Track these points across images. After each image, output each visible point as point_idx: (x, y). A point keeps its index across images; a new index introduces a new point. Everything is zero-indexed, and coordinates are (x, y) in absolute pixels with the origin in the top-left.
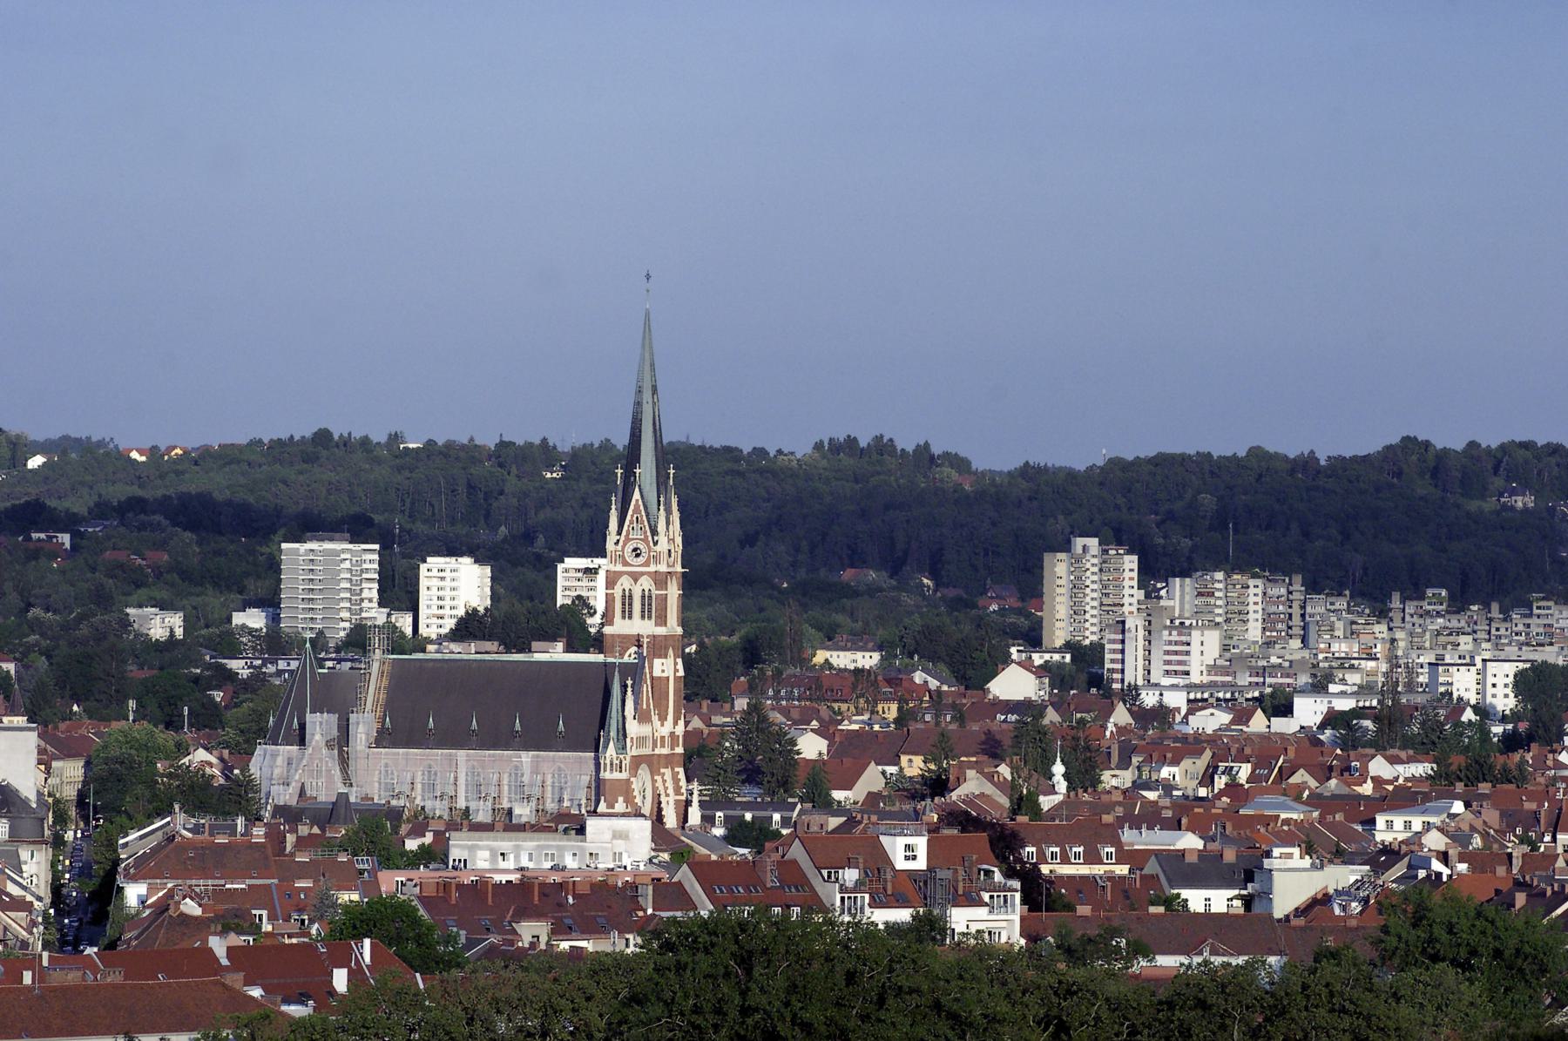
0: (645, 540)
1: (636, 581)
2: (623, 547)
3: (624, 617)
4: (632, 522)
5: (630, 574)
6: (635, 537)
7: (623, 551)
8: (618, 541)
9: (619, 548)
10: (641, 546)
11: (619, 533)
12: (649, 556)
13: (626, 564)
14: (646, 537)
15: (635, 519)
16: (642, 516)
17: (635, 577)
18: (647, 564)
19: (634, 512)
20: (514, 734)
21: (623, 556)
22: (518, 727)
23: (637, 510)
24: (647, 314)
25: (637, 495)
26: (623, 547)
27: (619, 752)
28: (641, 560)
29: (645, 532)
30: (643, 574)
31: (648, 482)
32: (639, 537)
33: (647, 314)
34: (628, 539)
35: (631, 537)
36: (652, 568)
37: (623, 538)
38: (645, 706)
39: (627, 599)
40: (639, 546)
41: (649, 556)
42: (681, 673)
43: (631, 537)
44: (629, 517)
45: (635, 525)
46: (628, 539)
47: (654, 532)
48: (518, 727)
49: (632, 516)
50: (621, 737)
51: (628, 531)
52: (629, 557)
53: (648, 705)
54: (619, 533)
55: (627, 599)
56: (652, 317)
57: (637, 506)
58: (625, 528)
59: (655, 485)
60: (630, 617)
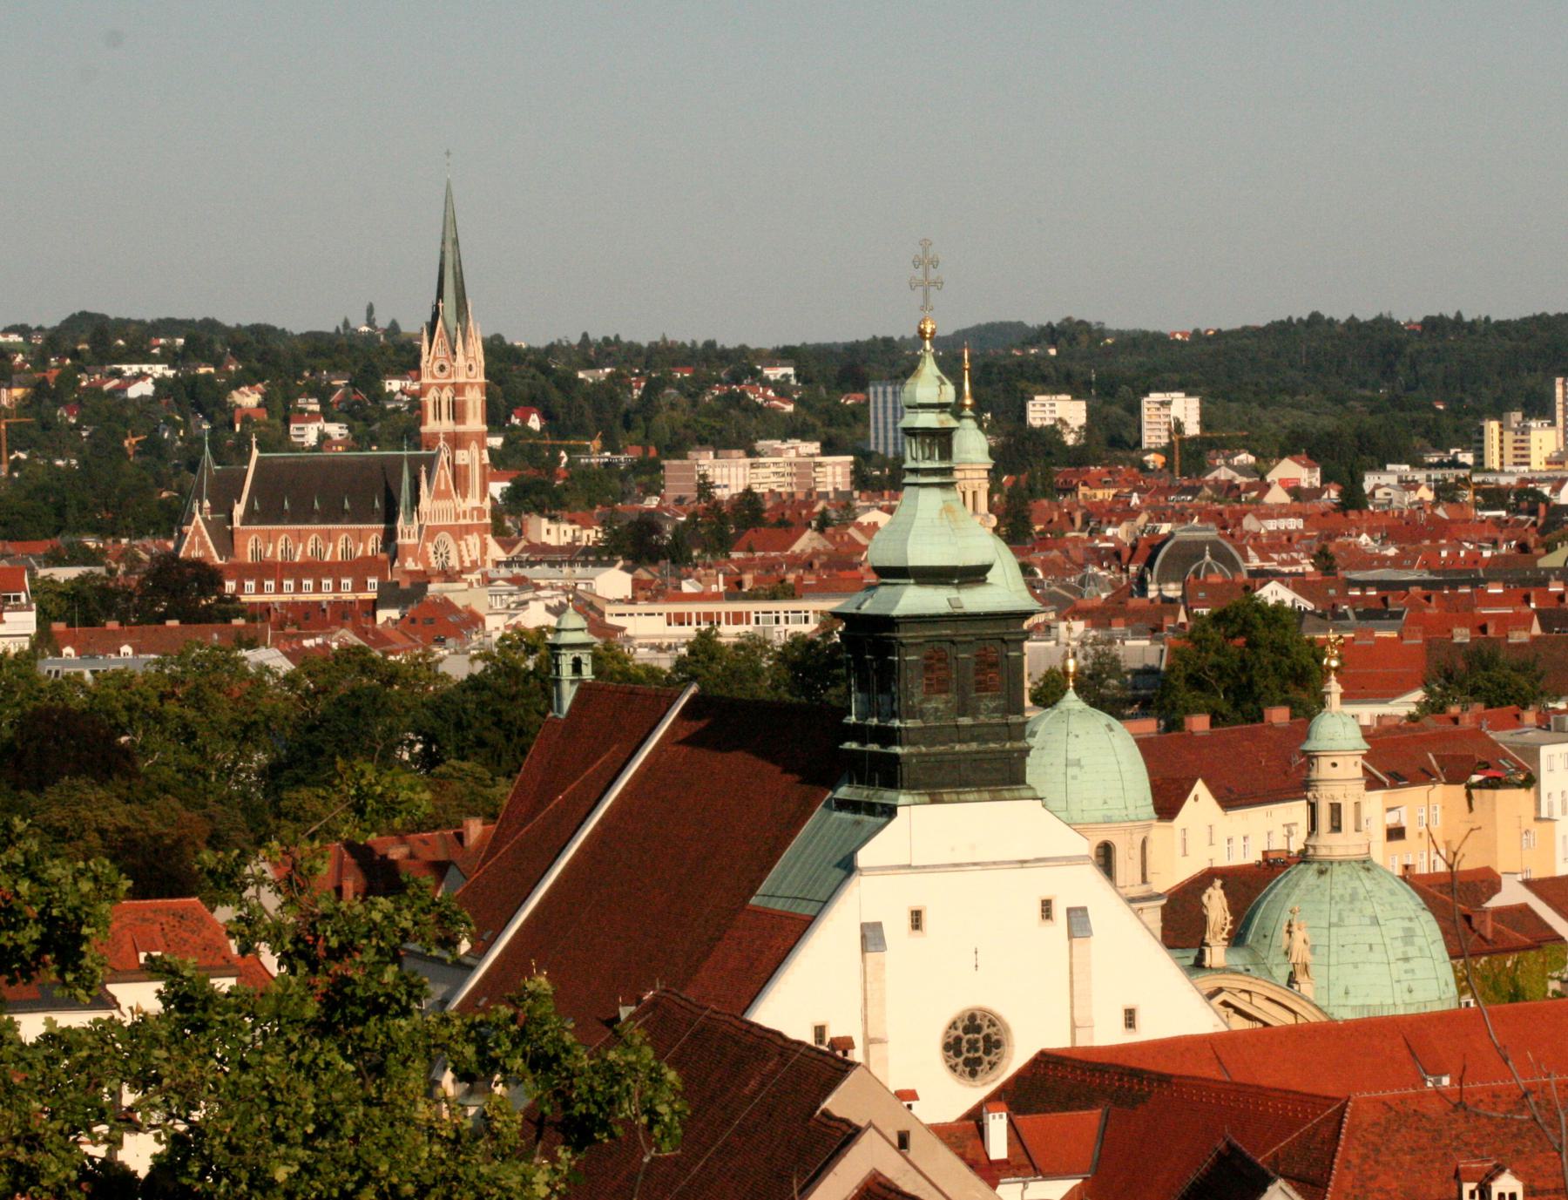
0: (447, 358)
1: (442, 389)
5: (438, 385)
10: (446, 363)
17: (441, 387)
18: (450, 376)
22: (347, 505)
24: (448, 188)
28: (445, 373)
30: (445, 384)
33: (448, 188)
34: (435, 358)
36: (452, 380)
39: (437, 404)
42: (487, 460)
46: (435, 358)
47: (454, 353)
55: (437, 404)
56: (454, 188)
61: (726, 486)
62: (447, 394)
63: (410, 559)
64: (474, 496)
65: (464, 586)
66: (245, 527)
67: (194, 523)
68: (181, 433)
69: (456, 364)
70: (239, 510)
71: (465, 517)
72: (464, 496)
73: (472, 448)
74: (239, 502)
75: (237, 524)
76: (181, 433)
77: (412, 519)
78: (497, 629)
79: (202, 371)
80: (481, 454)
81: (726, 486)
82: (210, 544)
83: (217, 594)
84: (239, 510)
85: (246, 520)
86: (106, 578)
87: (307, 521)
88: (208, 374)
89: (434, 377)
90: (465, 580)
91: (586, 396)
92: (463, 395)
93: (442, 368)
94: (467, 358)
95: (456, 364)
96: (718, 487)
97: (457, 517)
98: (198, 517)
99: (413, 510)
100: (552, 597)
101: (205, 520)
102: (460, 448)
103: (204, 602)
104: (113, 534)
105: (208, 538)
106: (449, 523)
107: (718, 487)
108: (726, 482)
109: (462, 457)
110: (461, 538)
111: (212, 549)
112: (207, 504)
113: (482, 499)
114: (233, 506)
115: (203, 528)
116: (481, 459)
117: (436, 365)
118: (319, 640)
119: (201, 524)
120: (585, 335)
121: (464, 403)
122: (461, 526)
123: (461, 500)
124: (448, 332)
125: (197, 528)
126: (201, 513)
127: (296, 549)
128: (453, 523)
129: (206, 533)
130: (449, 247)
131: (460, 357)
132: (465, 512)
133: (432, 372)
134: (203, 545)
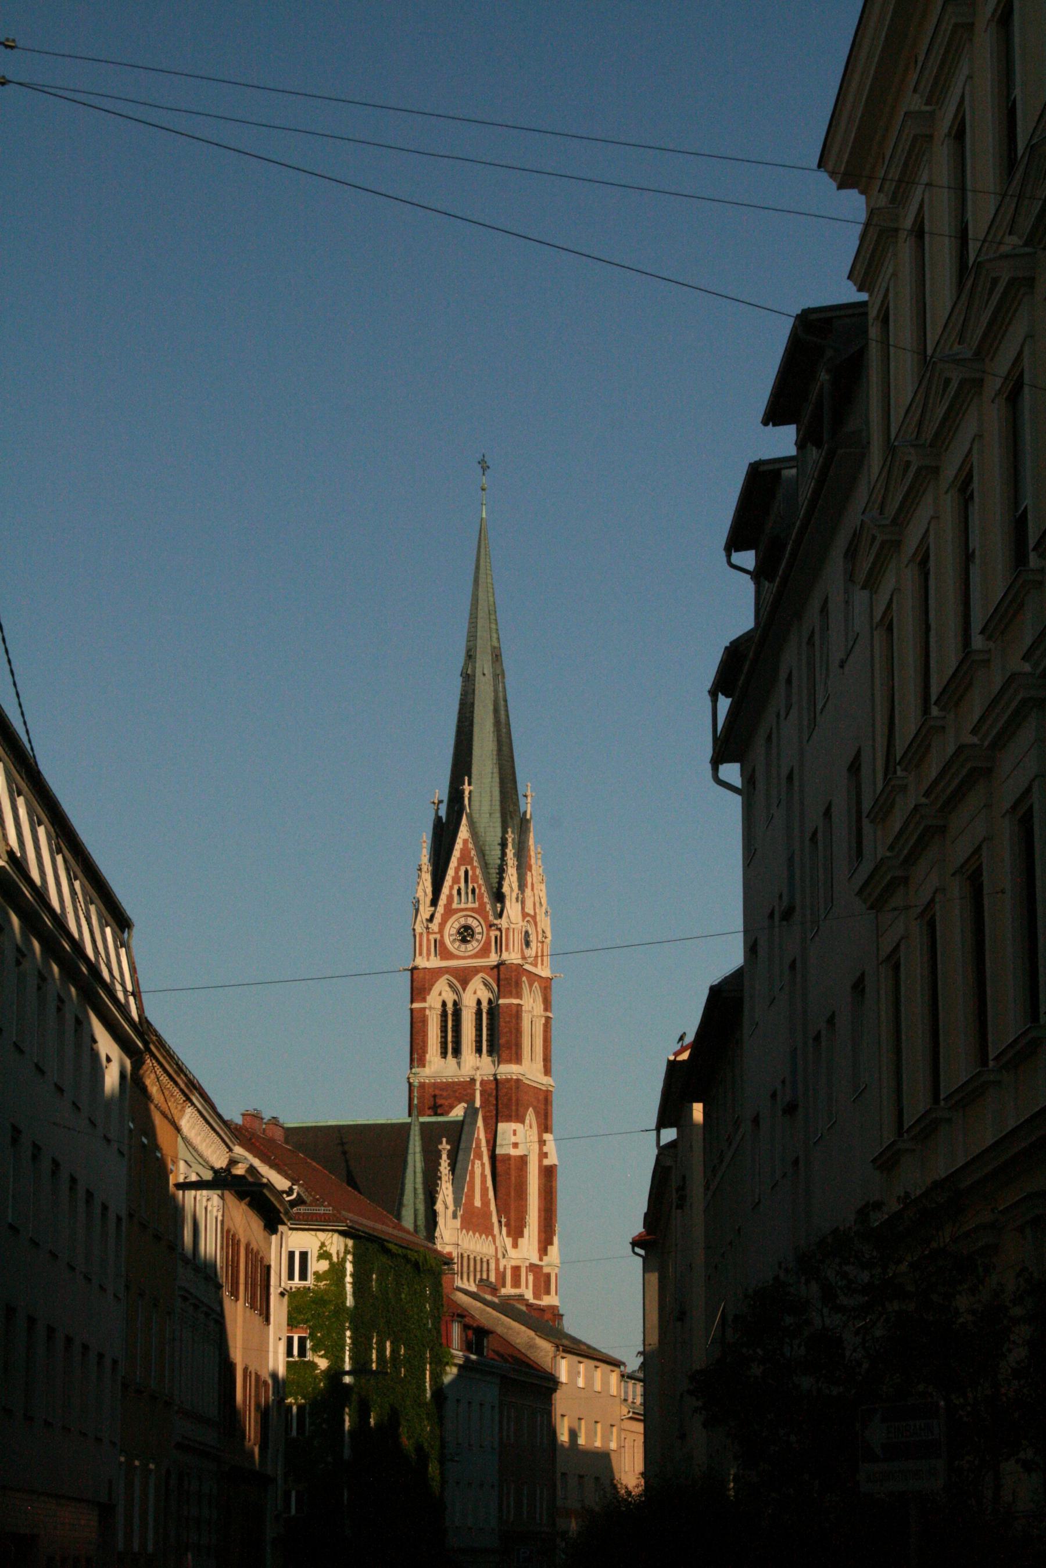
0: (481, 911)
1: (464, 983)
2: (442, 925)
4: (456, 880)
6: (463, 906)
7: (441, 931)
8: (432, 917)
9: (434, 926)
11: (434, 902)
12: (489, 938)
13: (446, 954)
14: (482, 905)
15: (462, 874)
16: (474, 869)
17: (463, 977)
18: (484, 952)
19: (462, 860)
21: (442, 943)
23: (464, 859)
25: (464, 833)
26: (442, 925)
28: (474, 946)
29: (481, 897)
30: (476, 970)
31: (486, 808)
32: (470, 905)
34: (449, 912)
35: (455, 906)
37: (440, 909)
38: (478, 1203)
39: (452, 1017)
40: (470, 921)
41: (489, 938)
43: (455, 906)
44: (451, 872)
45: (462, 885)
46: (449, 912)
49: (457, 870)
51: (450, 898)
52: (452, 946)
53: (485, 1202)
54: (434, 902)
55: (452, 1017)
57: (465, 852)
58: (445, 891)
59: (498, 815)
60: (457, 1052)
62: (477, 992)
69: (503, 923)
89: (444, 952)
92: (519, 996)
93: (466, 934)
95: (503, 923)
102: (509, 1119)
117: (453, 926)
121: (517, 1013)
123: (508, 1241)
124: (482, 854)
130: (484, 665)
131: (512, 909)
132: (516, 1270)
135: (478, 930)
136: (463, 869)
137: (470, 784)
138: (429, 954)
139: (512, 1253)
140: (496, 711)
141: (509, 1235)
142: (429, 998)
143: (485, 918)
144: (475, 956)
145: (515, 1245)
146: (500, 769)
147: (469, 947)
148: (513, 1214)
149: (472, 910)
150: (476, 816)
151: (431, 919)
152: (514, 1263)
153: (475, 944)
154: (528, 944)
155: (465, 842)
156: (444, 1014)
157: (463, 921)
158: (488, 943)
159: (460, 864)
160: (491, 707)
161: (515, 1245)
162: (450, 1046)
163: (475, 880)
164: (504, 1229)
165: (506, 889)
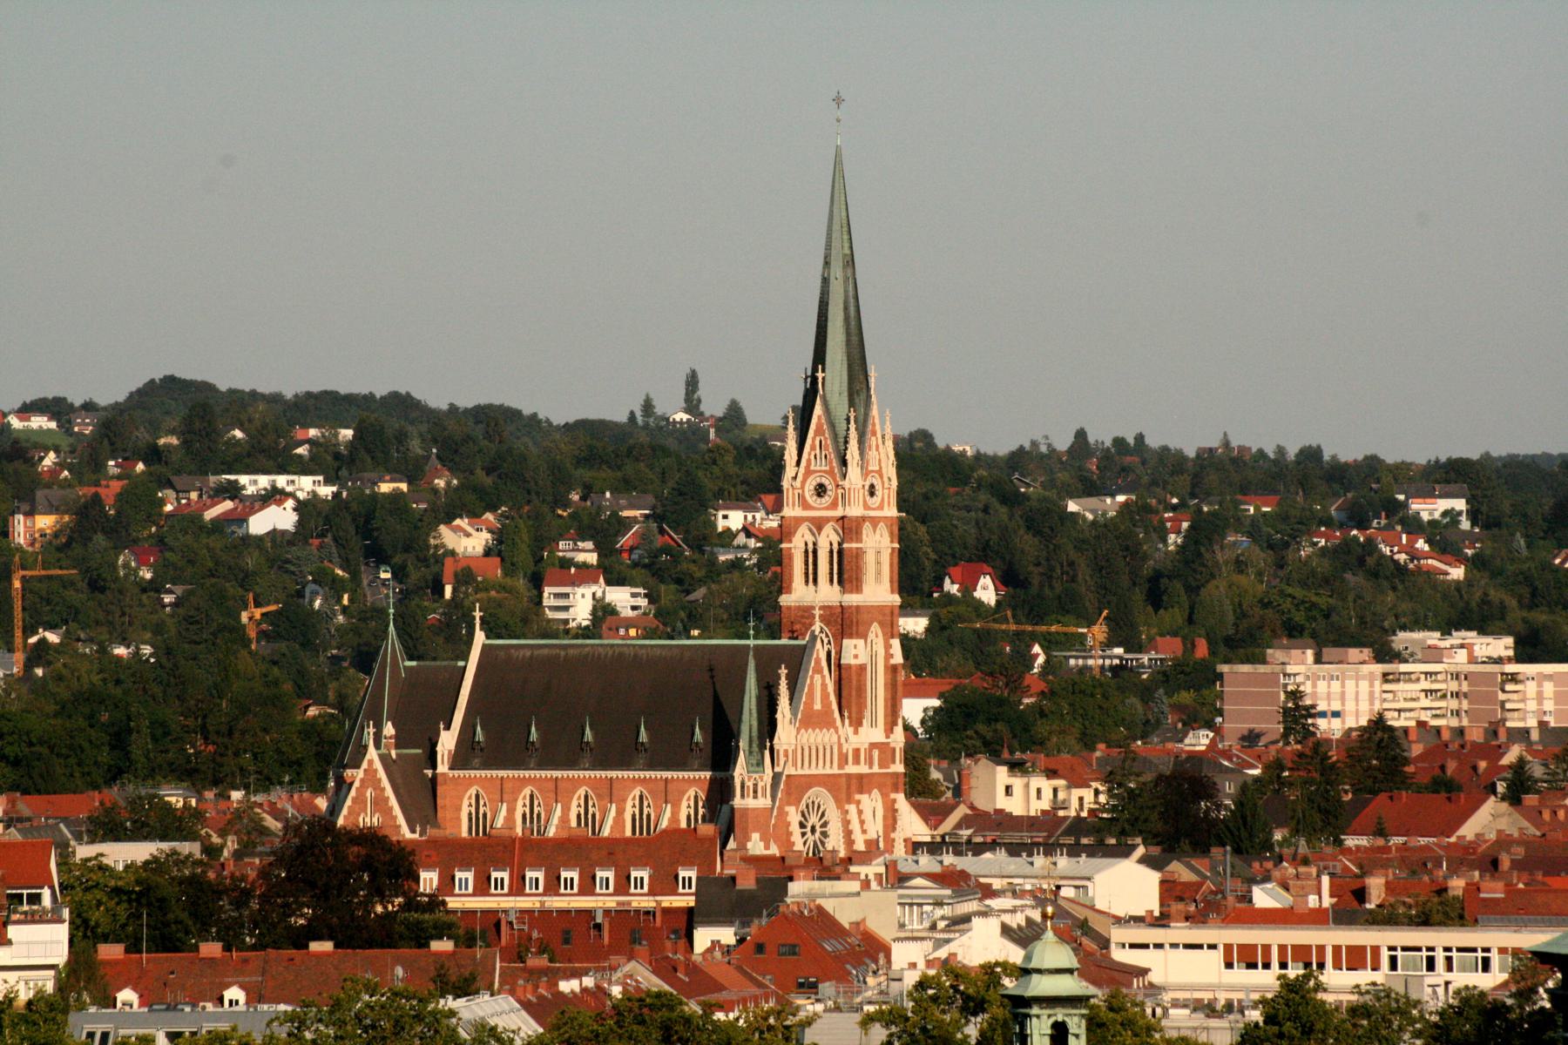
0: (831, 473)
1: (820, 529)
3: (807, 582)
4: (813, 447)
5: (812, 520)
6: (818, 468)
7: (803, 487)
9: (798, 484)
11: (798, 463)
12: (837, 494)
14: (832, 468)
17: (819, 524)
18: (834, 505)
19: (817, 432)
20: (582, 746)
21: (804, 497)
22: (643, 736)
23: (819, 431)
25: (818, 410)
27: (751, 769)
28: (826, 500)
29: (831, 462)
30: (828, 520)
31: (836, 388)
32: (824, 468)
34: (808, 472)
35: (812, 468)
39: (811, 555)
42: (898, 658)
43: (812, 468)
46: (808, 472)
47: (844, 463)
48: (643, 736)
50: (755, 748)
51: (809, 461)
52: (811, 498)
54: (798, 463)
55: (811, 555)
59: (846, 394)
60: (815, 581)
61: (1336, 714)
62: (829, 537)
63: (756, 836)
64: (873, 724)
65: (854, 886)
66: (456, 773)
67: (365, 765)
68: (345, 601)
69: (846, 484)
70: (447, 741)
71: (857, 761)
72: (857, 723)
73: (871, 636)
74: (448, 728)
75: (442, 768)
76: (345, 601)
77: (761, 763)
78: (913, 966)
79: (385, 488)
80: (888, 647)
81: (1336, 714)
82: (393, 801)
83: (404, 894)
84: (447, 741)
85: (461, 759)
86: (199, 863)
87: (571, 764)
88: (396, 496)
89: (805, 505)
90: (856, 876)
91: (1080, 545)
92: (859, 540)
93: (821, 490)
94: (865, 473)
95: (846, 484)
96: (1323, 714)
97: (843, 760)
98: (372, 753)
99: (762, 747)
100: (1013, 911)
101: (384, 759)
102: (851, 636)
103: (379, 909)
104: (216, 782)
105: (389, 792)
106: (828, 771)
107: (1323, 714)
108: (1336, 706)
109: (855, 651)
110: (849, 800)
111: (397, 811)
112: (389, 729)
113: (889, 730)
114: (438, 735)
115: (382, 774)
116: (889, 656)
118: (589, 982)
119: (378, 765)
120: (1081, 435)
121: (859, 554)
122: (849, 776)
123: (850, 730)
124: (832, 425)
125: (371, 772)
126: (377, 746)
127: (549, 813)
128: (836, 771)
129: (386, 783)
130: (837, 271)
131: (854, 471)
133: (802, 498)
134: (380, 804)
135: (829, 487)
136: (818, 439)
137: (823, 371)
138: (794, 505)
139: (852, 738)
140: (846, 308)
141: (851, 725)
142: (794, 540)
143: (835, 480)
144: (827, 508)
145: (856, 732)
146: (848, 357)
147: (823, 500)
148: (854, 709)
149: (824, 471)
150: (828, 396)
151: (795, 478)
152: (856, 746)
153: (827, 498)
154: (872, 494)
155: (819, 417)
156: (806, 552)
157: (818, 480)
158: (836, 499)
159: (816, 435)
160: (842, 306)
161: (856, 732)
162: (811, 577)
163: (827, 449)
164: (847, 721)
165: (848, 457)
